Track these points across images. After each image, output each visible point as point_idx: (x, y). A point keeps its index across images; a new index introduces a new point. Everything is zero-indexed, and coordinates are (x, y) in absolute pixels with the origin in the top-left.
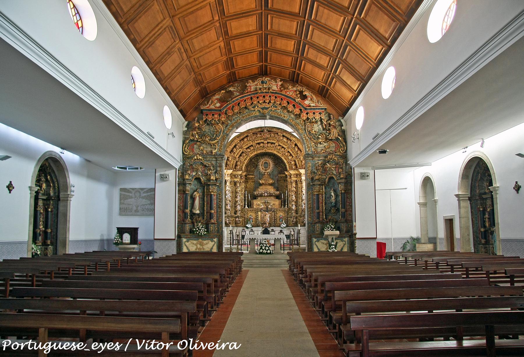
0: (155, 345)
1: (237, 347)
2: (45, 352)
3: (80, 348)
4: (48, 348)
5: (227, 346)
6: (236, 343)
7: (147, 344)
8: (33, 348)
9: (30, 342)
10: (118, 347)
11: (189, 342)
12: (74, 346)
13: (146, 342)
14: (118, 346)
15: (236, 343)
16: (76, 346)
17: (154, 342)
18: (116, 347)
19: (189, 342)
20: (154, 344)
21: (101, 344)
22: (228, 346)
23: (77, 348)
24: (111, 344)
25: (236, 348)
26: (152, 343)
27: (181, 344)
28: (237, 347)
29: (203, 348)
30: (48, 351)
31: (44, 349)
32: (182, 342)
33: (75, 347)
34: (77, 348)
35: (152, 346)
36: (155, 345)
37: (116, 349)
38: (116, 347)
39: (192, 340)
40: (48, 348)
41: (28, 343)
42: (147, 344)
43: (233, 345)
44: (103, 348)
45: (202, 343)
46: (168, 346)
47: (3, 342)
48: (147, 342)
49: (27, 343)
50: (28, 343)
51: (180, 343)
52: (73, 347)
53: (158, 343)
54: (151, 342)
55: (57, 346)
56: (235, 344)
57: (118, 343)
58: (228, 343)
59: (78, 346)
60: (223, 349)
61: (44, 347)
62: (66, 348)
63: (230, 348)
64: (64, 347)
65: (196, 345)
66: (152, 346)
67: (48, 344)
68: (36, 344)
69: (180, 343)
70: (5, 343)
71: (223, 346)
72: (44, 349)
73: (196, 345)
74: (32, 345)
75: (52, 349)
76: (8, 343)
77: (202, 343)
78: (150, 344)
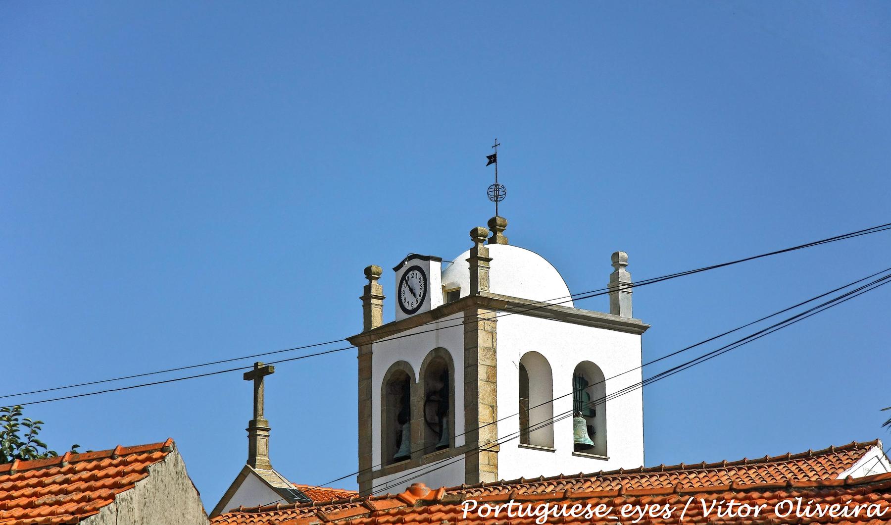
1: (881, 513)
2: (537, 521)
4: (544, 514)
8: (515, 514)
10: (669, 513)
11: (795, 503)
12: (590, 510)
14: (668, 510)
16: (593, 511)
19: (795, 503)
20: (733, 506)
23: (594, 514)
26: (729, 506)
27: (782, 507)
28: (881, 513)
29: (821, 515)
31: (535, 517)
32: (782, 503)
33: (591, 513)
34: (594, 514)
35: (729, 510)
40: (544, 514)
41: (508, 506)
42: (720, 507)
44: (642, 515)
49: (505, 506)
50: (508, 506)
51: (780, 505)
52: (587, 512)
54: (727, 504)
58: (865, 506)
59: (597, 510)
61: (536, 512)
62: (576, 514)
64: (572, 511)
65: (808, 509)
67: (542, 508)
69: (780, 505)
70: (467, 505)
72: (535, 517)
73: (808, 509)
75: (550, 516)
76: (471, 504)
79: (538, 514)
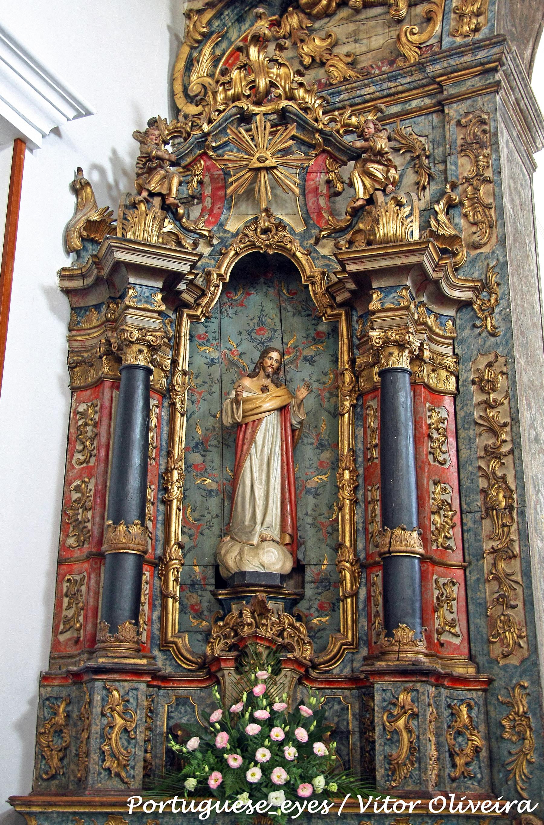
0: (390, 806)
3: (261, 809)
5: (515, 807)
6: (529, 801)
7: (376, 804)
8: (179, 809)
9: (176, 799)
10: (327, 809)
13: (374, 801)
14: (326, 806)
15: (529, 801)
17: (387, 800)
18: (323, 807)
21: (297, 804)
22: (515, 806)
24: (314, 803)
25: (529, 810)
27: (436, 803)
30: (206, 814)
33: (252, 809)
34: (255, 809)
35: (385, 806)
36: (390, 806)
37: (322, 812)
38: (323, 807)
39: (453, 796)
42: (376, 804)
43: (524, 805)
44: (301, 811)
45: (470, 801)
46: (412, 805)
47: (128, 800)
48: (377, 799)
53: (394, 802)
55: (221, 806)
56: (528, 803)
57: (326, 802)
58: (516, 802)
59: (258, 806)
60: (507, 811)
61: (199, 808)
63: (520, 811)
65: (461, 805)
66: (385, 806)
68: (184, 803)
70: (133, 801)
71: (508, 807)
72: (199, 813)
73: (461, 805)
74: (179, 805)
75: (213, 811)
77: (470, 801)
78: (380, 805)
79: (201, 810)
